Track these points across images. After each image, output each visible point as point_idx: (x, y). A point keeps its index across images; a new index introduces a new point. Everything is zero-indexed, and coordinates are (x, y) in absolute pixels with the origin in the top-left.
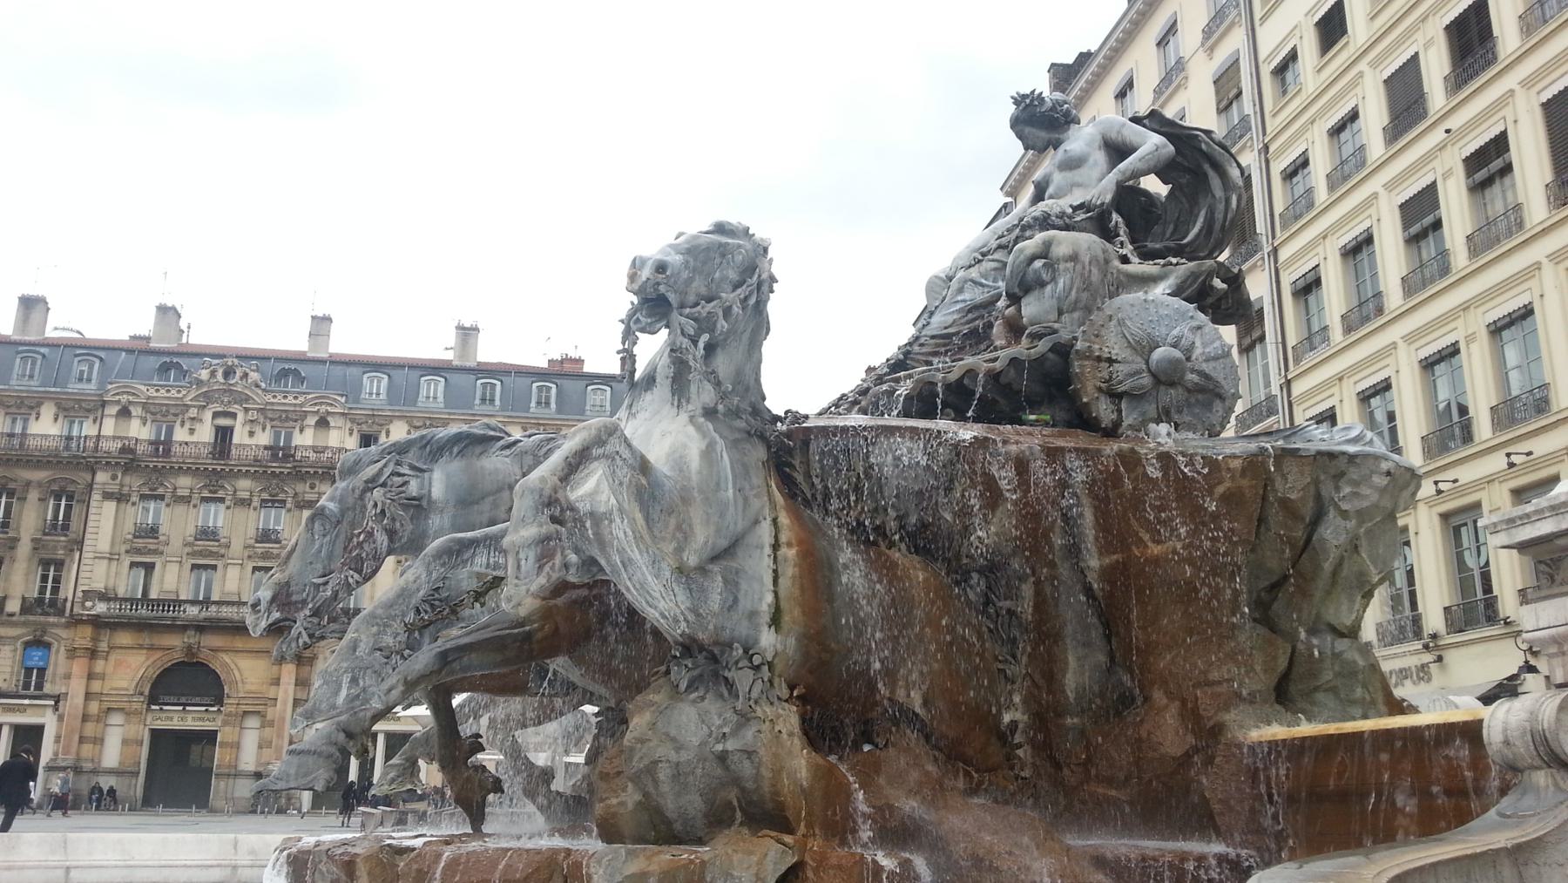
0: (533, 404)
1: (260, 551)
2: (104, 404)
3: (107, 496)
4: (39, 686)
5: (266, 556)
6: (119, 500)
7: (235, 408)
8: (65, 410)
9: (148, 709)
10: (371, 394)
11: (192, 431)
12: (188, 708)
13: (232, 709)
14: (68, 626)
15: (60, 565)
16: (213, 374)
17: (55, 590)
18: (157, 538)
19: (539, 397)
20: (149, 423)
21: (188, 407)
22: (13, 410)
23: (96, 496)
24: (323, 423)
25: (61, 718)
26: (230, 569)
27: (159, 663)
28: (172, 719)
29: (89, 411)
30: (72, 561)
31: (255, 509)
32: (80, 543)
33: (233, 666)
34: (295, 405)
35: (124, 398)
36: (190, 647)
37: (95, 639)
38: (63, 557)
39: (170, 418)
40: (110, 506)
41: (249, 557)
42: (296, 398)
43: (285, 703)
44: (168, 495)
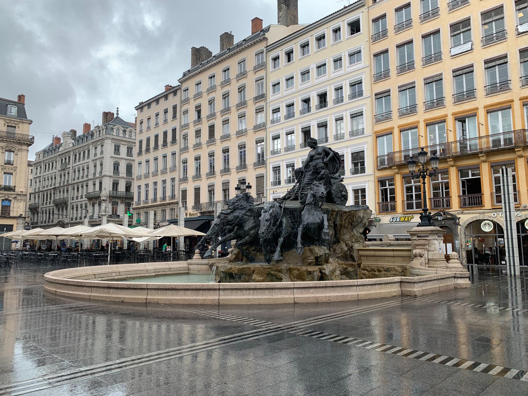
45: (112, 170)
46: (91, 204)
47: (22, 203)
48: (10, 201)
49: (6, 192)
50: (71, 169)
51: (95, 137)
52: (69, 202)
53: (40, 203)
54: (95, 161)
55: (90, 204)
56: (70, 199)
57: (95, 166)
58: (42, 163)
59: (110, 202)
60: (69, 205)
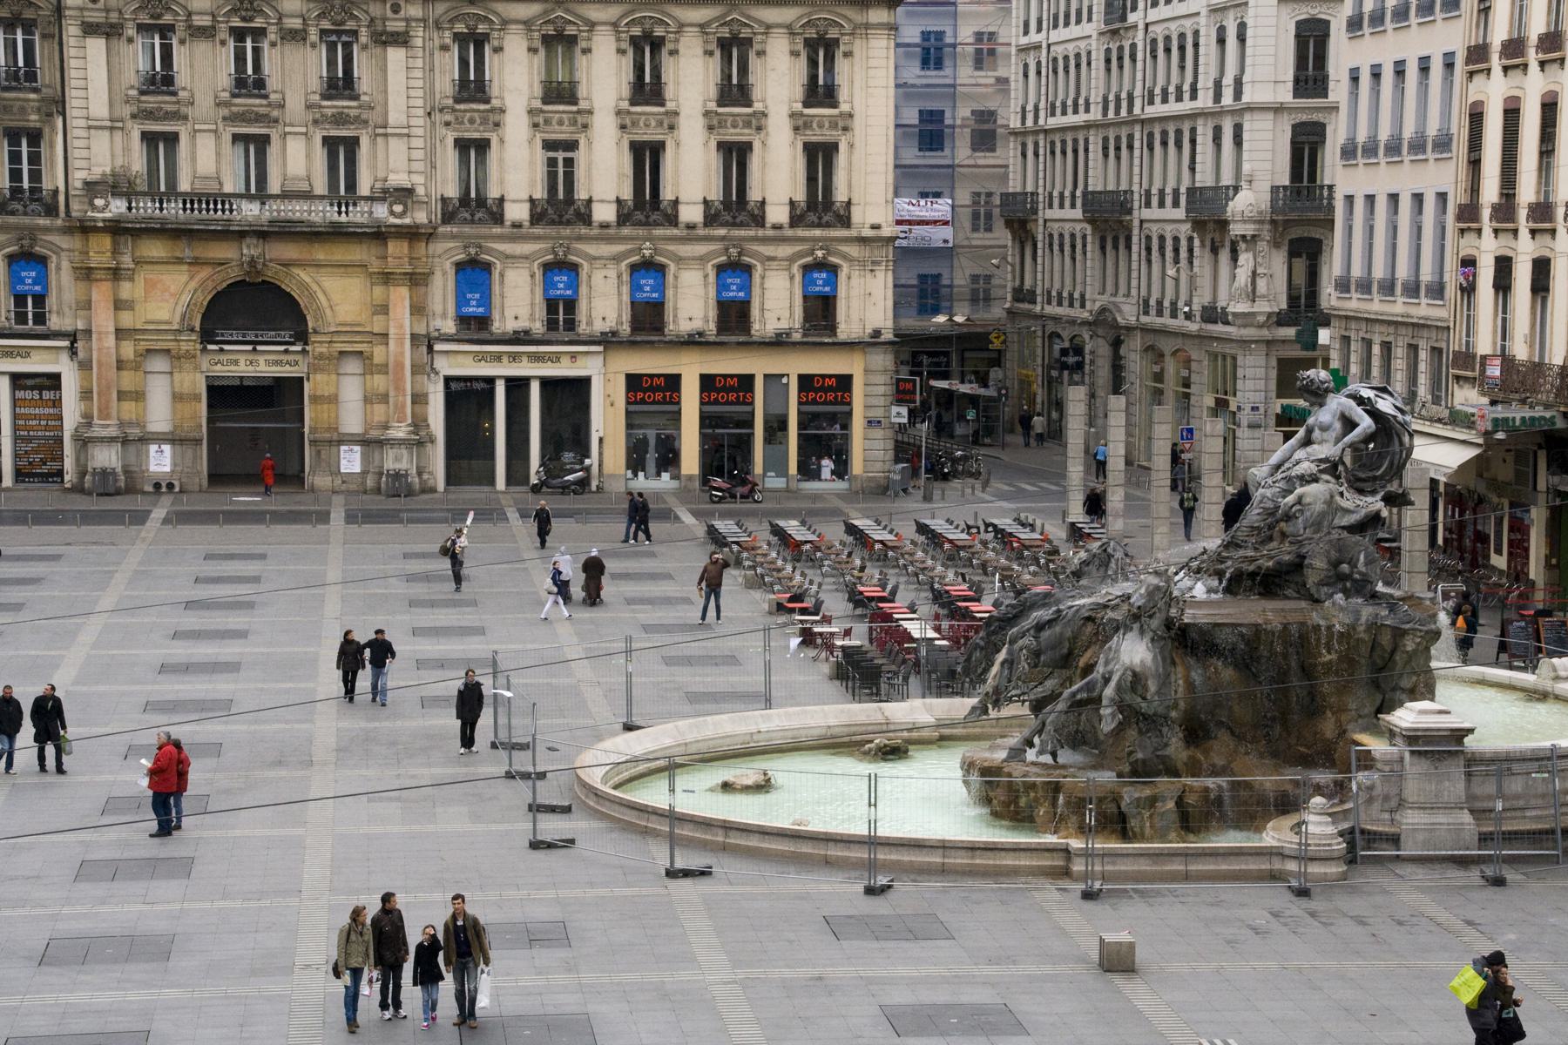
1: (329, 112)
3: (90, 29)
4: (40, 318)
5: (340, 119)
6: (108, 36)
9: (204, 350)
12: (259, 348)
13: (323, 349)
14: (68, 231)
15: (35, 137)
17: (36, 176)
18: (174, 94)
23: (72, 30)
25: (85, 366)
26: (290, 141)
27: (210, 285)
28: (236, 362)
30: (53, 129)
31: (313, 46)
32: (58, 104)
33: (315, 287)
36: (252, 262)
37: (116, 252)
38: (38, 125)
40: (97, 46)
41: (316, 122)
43: (401, 340)
44: (180, 26)
45: (1290, 75)
46: (1208, 243)
47: (880, 275)
48: (833, 270)
49: (817, 232)
50: (1140, 34)
52: (1136, 213)
53: (1040, 190)
54: (1219, 16)
55: (1203, 245)
56: (1136, 197)
57: (1221, 41)
59: (1276, 244)
60: (1136, 231)
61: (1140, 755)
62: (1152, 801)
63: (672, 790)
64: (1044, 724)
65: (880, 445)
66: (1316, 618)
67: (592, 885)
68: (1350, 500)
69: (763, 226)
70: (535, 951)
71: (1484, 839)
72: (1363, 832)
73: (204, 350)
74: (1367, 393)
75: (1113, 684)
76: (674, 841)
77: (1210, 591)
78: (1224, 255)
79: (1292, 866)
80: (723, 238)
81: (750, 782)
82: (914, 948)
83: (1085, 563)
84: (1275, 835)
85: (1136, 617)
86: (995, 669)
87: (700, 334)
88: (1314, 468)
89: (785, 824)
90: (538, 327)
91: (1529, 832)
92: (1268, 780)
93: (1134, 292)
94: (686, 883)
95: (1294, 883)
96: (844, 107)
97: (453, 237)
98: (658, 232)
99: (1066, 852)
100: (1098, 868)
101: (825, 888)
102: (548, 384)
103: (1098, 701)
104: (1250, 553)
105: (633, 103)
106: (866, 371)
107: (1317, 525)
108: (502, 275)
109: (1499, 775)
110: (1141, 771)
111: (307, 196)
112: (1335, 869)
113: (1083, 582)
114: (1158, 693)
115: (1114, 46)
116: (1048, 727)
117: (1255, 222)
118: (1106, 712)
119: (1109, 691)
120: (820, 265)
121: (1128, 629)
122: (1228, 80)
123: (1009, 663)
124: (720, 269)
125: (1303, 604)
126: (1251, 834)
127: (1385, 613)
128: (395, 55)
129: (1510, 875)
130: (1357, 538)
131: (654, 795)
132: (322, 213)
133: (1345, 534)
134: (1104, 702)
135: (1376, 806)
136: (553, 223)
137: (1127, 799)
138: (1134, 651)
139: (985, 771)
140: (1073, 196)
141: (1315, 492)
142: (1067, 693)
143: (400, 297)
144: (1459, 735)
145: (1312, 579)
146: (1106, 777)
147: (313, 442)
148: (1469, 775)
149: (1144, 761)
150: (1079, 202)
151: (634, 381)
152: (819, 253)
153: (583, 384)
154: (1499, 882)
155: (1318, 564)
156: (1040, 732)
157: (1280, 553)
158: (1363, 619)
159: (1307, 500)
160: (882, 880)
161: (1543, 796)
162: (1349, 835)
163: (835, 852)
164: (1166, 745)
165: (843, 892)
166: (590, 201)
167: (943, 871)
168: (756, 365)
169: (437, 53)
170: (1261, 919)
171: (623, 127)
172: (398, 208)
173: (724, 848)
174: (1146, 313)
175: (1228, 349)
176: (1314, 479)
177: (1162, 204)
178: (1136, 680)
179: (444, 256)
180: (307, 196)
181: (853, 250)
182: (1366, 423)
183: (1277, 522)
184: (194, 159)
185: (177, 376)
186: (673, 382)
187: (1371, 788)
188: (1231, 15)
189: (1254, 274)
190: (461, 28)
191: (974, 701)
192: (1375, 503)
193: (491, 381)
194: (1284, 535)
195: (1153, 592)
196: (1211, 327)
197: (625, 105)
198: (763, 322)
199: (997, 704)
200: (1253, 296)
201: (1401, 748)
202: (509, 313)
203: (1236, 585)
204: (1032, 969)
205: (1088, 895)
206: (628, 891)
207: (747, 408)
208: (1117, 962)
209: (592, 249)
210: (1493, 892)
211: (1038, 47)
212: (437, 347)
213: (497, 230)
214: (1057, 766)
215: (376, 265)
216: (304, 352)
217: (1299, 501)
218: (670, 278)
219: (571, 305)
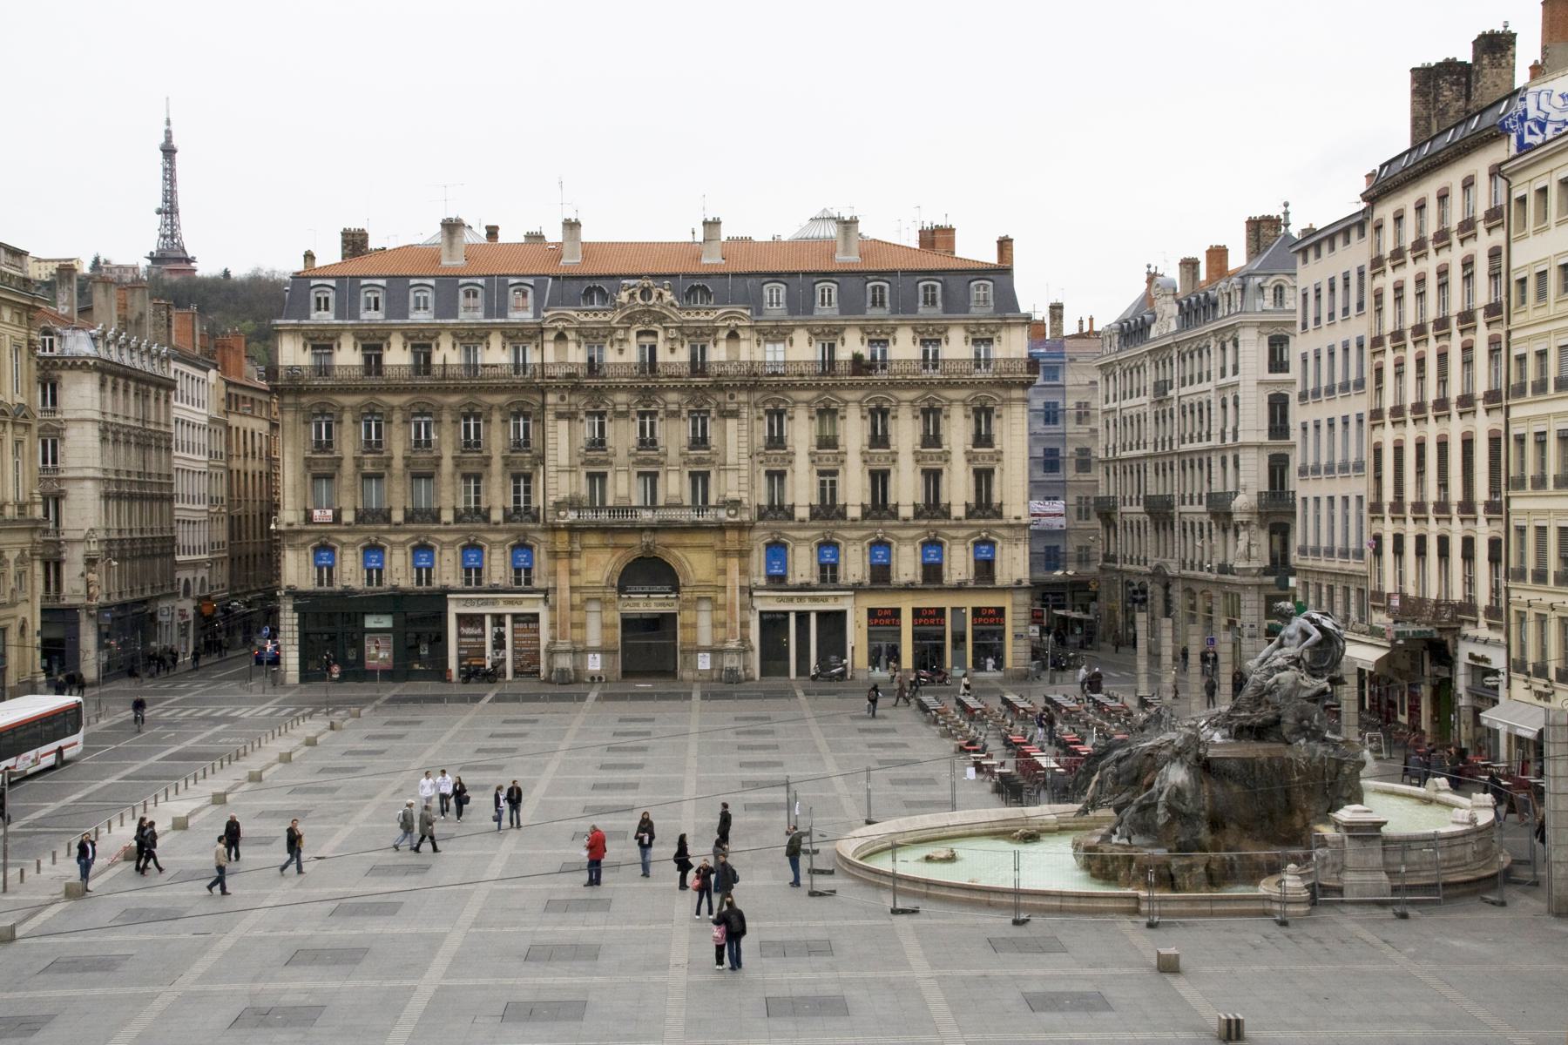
0: (921, 304)
1: (693, 457)
2: (542, 331)
3: (560, 416)
4: (528, 582)
5: (699, 461)
6: (569, 419)
7: (655, 327)
8: (510, 338)
9: (620, 598)
10: (771, 304)
11: (621, 351)
13: (686, 596)
14: (545, 530)
15: (528, 478)
16: (632, 296)
17: (528, 500)
18: (605, 450)
19: (926, 296)
20: (583, 345)
21: (615, 330)
22: (466, 341)
23: (550, 417)
24: (733, 336)
25: (553, 609)
27: (623, 560)
28: (638, 605)
29: (530, 337)
30: (538, 472)
31: (684, 420)
32: (541, 459)
34: (708, 321)
35: (560, 325)
36: (648, 545)
37: (571, 542)
39: (600, 339)
40: (563, 425)
41: (685, 463)
42: (707, 314)
44: (610, 412)
45: (1265, 425)
48: (992, 544)
49: (982, 522)
50: (1176, 402)
51: (1220, 314)
55: (1217, 527)
57: (1224, 407)
58: (1118, 368)
59: (1262, 527)
60: (1176, 519)
61: (1182, 839)
62: (1190, 868)
63: (894, 861)
64: (1122, 819)
65: (1022, 649)
66: (1289, 754)
67: (846, 918)
68: (1308, 681)
69: (949, 518)
70: (813, 958)
71: (1395, 890)
72: (1320, 886)
73: (620, 598)
74: (1316, 616)
75: (1164, 795)
76: (895, 892)
77: (1223, 737)
78: (1231, 534)
79: (1277, 907)
80: (925, 526)
81: (942, 856)
82: (1043, 958)
83: (1146, 721)
84: (1266, 888)
85: (1178, 754)
86: (1092, 786)
87: (913, 583)
88: (1285, 662)
89: (965, 881)
90: (815, 581)
91: (1422, 885)
92: (1262, 853)
93: (1176, 556)
94: (904, 917)
95: (1278, 918)
96: (997, 447)
97: (765, 528)
98: (887, 523)
99: (1137, 898)
100: (1156, 909)
101: (990, 921)
102: (822, 615)
103: (1155, 805)
104: (1247, 714)
105: (871, 447)
106: (1014, 605)
107: (1288, 697)
108: (793, 550)
109: (1403, 850)
110: (1183, 848)
111: (680, 506)
112: (1302, 909)
113: (1146, 732)
114: (1193, 800)
115: (1160, 410)
116: (1125, 822)
117: (1252, 513)
118: (1161, 811)
119: (1163, 798)
120: (985, 542)
121: (1173, 761)
122: (1229, 429)
123: (1100, 783)
124: (924, 544)
125: (1281, 745)
126: (1251, 888)
127: (1331, 750)
128: (731, 424)
129: (1411, 912)
130: (1311, 705)
131: (883, 864)
132: (687, 516)
133: (1305, 702)
134: (1160, 805)
135: (1328, 870)
136: (823, 519)
137: (1174, 866)
138: (1177, 775)
139: (1088, 849)
140: (1138, 498)
141: (1286, 676)
142: (1136, 800)
143: (734, 564)
144: (1378, 826)
145: (1286, 730)
146: (1161, 852)
147: (682, 652)
148: (1384, 850)
149: (1185, 843)
150: (1142, 502)
151: (872, 613)
152: (984, 534)
153: (840, 616)
154: (1404, 916)
155: (1289, 721)
156: (1120, 824)
157: (1266, 714)
158: (1318, 753)
159: (1281, 681)
160: (1023, 916)
161: (1430, 863)
162: (1312, 888)
163: (994, 898)
164: (1198, 833)
165: (999, 923)
166: (845, 505)
167: (1061, 911)
168: (946, 602)
169: (756, 423)
170: (1258, 940)
171: (865, 461)
172: (732, 512)
173: (927, 896)
174: (1184, 568)
175: (1235, 590)
176: (1285, 669)
177: (1192, 503)
178: (1179, 792)
179: (759, 540)
180: (680, 506)
181: (1005, 532)
182: (1316, 634)
183: (1261, 697)
184: (615, 487)
185: (604, 614)
186: (896, 613)
187: (1325, 858)
188: (1230, 391)
189: (1249, 545)
190: (769, 406)
191: (1078, 806)
192: (1323, 683)
193: (786, 613)
194: (1268, 703)
195: (1188, 738)
196: (1224, 577)
197: (866, 448)
198: (950, 575)
199: (1094, 807)
200: (1249, 558)
201: (1343, 834)
202: (798, 574)
203: (1242, 732)
204: (1116, 971)
205: (1151, 925)
206: (868, 922)
207: (940, 628)
208: (1169, 966)
209: (847, 534)
210: (1403, 922)
211: (1114, 410)
212: (755, 594)
213: (790, 524)
214: (1131, 846)
215: (719, 545)
216: (677, 598)
217: (1277, 682)
218: (894, 550)
219: (834, 567)
